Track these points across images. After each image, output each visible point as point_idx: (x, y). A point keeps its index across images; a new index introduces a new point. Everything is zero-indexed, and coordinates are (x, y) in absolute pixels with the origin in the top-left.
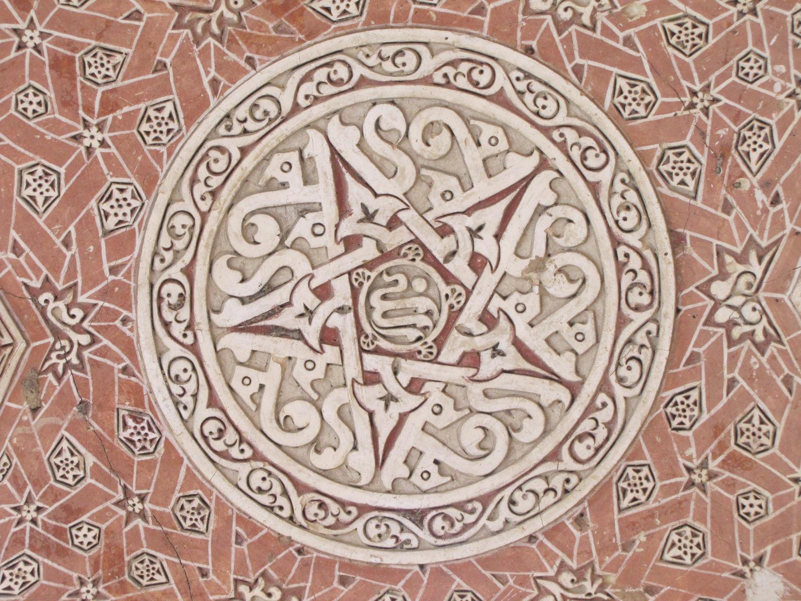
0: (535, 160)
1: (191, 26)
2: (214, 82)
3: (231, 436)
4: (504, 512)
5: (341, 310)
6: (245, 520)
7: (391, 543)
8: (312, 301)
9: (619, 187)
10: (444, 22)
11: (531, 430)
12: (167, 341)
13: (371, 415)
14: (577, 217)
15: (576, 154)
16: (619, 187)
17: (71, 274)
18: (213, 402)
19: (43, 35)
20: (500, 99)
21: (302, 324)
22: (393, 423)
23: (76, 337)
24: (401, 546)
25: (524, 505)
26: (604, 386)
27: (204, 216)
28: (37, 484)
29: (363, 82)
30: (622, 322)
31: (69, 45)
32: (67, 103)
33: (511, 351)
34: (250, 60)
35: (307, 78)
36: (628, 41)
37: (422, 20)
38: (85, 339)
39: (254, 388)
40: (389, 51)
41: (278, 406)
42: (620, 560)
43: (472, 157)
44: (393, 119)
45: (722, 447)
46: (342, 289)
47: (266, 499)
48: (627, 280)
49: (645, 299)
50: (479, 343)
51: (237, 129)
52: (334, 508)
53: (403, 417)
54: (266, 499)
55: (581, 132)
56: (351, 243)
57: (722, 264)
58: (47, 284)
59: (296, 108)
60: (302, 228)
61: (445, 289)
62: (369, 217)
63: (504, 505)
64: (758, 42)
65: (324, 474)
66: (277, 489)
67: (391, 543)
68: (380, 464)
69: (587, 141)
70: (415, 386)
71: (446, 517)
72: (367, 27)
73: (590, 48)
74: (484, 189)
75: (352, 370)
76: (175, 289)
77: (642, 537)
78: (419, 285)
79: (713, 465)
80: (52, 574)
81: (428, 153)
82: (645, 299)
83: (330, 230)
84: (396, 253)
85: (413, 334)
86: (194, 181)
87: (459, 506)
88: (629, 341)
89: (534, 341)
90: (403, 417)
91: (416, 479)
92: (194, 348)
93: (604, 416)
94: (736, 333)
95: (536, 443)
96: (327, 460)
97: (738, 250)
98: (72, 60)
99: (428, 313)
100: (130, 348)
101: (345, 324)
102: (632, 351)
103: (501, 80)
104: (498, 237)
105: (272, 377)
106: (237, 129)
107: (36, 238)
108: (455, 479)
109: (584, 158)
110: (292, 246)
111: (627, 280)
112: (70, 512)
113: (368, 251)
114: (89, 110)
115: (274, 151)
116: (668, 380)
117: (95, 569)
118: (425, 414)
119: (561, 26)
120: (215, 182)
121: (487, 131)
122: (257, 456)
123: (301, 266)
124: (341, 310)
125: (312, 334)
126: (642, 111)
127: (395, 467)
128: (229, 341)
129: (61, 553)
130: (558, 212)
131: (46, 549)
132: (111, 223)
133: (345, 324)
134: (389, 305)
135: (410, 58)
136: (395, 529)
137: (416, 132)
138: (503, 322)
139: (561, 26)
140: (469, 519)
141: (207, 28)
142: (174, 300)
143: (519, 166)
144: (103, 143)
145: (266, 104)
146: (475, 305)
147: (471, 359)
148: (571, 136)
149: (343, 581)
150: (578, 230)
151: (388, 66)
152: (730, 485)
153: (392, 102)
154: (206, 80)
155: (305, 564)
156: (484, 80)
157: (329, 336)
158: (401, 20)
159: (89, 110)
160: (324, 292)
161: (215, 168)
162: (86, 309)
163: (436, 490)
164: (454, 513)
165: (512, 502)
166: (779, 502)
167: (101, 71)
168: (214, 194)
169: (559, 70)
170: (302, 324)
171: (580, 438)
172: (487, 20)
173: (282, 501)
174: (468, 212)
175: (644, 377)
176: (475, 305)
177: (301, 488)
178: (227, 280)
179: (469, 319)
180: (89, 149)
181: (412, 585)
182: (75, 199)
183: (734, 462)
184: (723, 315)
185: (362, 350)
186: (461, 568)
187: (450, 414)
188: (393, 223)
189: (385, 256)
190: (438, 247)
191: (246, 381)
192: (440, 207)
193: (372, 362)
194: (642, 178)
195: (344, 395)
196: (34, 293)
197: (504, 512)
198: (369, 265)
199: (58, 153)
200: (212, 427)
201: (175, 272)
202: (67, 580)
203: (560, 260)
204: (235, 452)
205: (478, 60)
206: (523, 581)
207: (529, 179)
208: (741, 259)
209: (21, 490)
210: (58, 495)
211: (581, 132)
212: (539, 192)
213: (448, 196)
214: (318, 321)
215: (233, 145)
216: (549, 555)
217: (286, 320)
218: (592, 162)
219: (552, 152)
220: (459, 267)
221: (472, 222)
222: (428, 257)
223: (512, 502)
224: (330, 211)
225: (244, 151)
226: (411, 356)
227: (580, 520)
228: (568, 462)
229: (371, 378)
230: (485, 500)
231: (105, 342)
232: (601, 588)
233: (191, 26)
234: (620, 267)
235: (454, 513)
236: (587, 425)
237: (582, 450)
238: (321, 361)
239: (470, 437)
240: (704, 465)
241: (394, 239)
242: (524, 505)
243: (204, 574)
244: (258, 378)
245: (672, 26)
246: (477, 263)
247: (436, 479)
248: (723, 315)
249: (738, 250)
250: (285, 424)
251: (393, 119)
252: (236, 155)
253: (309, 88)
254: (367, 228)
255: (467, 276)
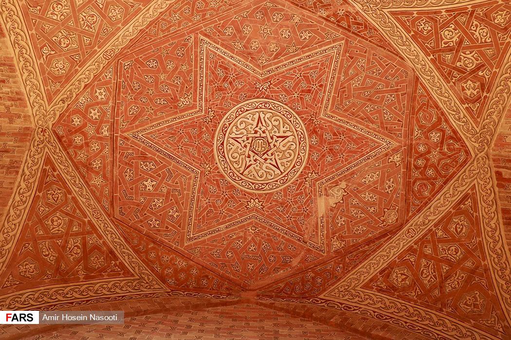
0: (283, 171)
1: (313, 115)
2: (303, 117)
3: (240, 113)
4: (222, 159)
5: (260, 134)
6: (226, 114)
7: (218, 139)
8: (262, 130)
9: (276, 185)
10: (309, 158)
11: (236, 166)
12: (259, 103)
13: (241, 138)
14: (272, 178)
15: (283, 178)
16: (276, 185)
17: (272, 88)
18: (247, 110)
19: (315, 89)
20: (294, 166)
21: (259, 127)
22: (239, 141)
23: (261, 87)
24: (217, 140)
25: (222, 163)
26: (242, 179)
27: (280, 113)
28: (236, 78)
29: (300, 143)
30: (253, 184)
31: (312, 93)
32: (303, 91)
33: (250, 163)
34: (306, 124)
35: (302, 134)
36: (301, 189)
37: (309, 154)
38: (261, 89)
39: (248, 118)
40: (305, 148)
41: (245, 122)
42: (211, 178)
43: (285, 161)
44: (293, 147)
45: (229, 198)
46: (264, 135)
47: (229, 118)
48: (260, 185)
49: (256, 188)
50: (252, 158)
51: (294, 120)
52: (226, 129)
53: (240, 143)
54: (229, 118)
55: (287, 180)
56: (272, 138)
57: (261, 201)
58: (271, 84)
59: (297, 131)
60: (276, 129)
61: (262, 153)
62: (276, 141)
63: (223, 159)
64: (299, 211)
65: (232, 128)
66: (230, 120)
67: (218, 139)
68: (232, 138)
69: (285, 180)
70: (245, 146)
71: (222, 149)
72: (310, 145)
73: (301, 183)
74: (279, 162)
75: (249, 135)
76: (268, 106)
77: (215, 182)
78: (263, 149)
79: (226, 196)
80: (220, 79)
81: (286, 153)
82: (256, 188)
83: (275, 134)
84: (269, 146)
85: (255, 147)
86: (286, 112)
87: (223, 152)
88: (249, 185)
89: (251, 168)
90: (240, 143)
91: (229, 144)
92: (257, 108)
93: (237, 179)
94: (249, 203)
95: (233, 166)
96: (234, 129)
97: (263, 204)
98: (310, 93)
99: (258, 150)
100: (258, 97)
101: (258, 135)
102: (248, 184)
103: (297, 167)
104: (270, 164)
105: (250, 121)
106: (294, 120)
107: (279, 83)
108: (228, 151)
109: (282, 180)
110: (273, 127)
111: (260, 185)
112: (231, 83)
113: (270, 140)
114: (301, 95)
115: (290, 126)
116: (242, 191)
117: (220, 86)
118: (240, 147)
119: (305, 178)
120: (286, 115)
121: (289, 164)
122: (236, 117)
123: (269, 128)
124: (260, 134)
125: (257, 129)
126: (289, 190)
127: (232, 141)
128: (257, 114)
129: (224, 81)
130: (273, 174)
131: (225, 78)
132: (280, 96)
133: (258, 135)
134: (260, 143)
135: (303, 152)
136: (220, 140)
137: (290, 151)
138: (255, 163)
139: (305, 178)
140: (221, 153)
141: (312, 117)
142: (266, 106)
143: (282, 168)
144: (295, 97)
145: (298, 125)
146: (258, 158)
147: (249, 157)
148: (286, 178)
149: (212, 130)
150: (270, 177)
151: (302, 148)
152: (223, 199)
153: (296, 147)
154: (303, 116)
155: (216, 123)
156: (298, 164)
157: (256, 132)
158: (310, 150)
159: (301, 95)
160: (264, 132)
161: (288, 116)
162: (266, 90)
163: (227, 148)
164: (222, 150)
165: (223, 161)
166: (219, 207)
167: (308, 98)
168: (283, 115)
169: (298, 177)
170: (259, 127)
171: (233, 174)
172: (308, 166)
173: (228, 120)
174: (275, 159)
175: (243, 186)
176: (258, 158)
177: (230, 124)
178: (268, 115)
179: (256, 157)
180: (294, 94)
181: (210, 142)
182: (286, 90)
183: (227, 200)
184: (252, 200)
185: (253, 137)
186: (212, 150)
187: (240, 151)
188: (275, 146)
189: (269, 143)
190: (269, 153)
191: (250, 116)
192: (276, 154)
193: (251, 139)
194: (278, 189)
195: (245, 134)
196: (270, 82)
197: (222, 159)
198: (268, 141)
199: (294, 88)
200: (243, 109)
201: (271, 106)
202: (219, 81)
203: (265, 174)
204: (238, 113)
205: (301, 164)
206: (209, 161)
207: (280, 170)
208: (262, 205)
209: (236, 75)
210: (234, 81)
211: (287, 180)
212: (277, 171)
213: (278, 155)
214: (259, 130)
215: (292, 119)
216: (214, 166)
217: (260, 124)
218: (281, 181)
219: (284, 174)
220: (265, 156)
221: (273, 159)
222: (268, 151)
223: (223, 161)
224: (277, 134)
225: (290, 121)
226: (251, 146)
227: (218, 172)
228: (229, 171)
229: (248, 139)
230: (224, 156)
231: (260, 93)
232: (207, 175)
233: (313, 115)
234: (262, 184)
235: (222, 150)
236: (235, 175)
237: (231, 174)
238: (252, 130)
239: (235, 155)
240: (226, 195)
241: (272, 145)
242: (222, 163)
243: (217, 105)
244: (250, 119)
245: (303, 197)
246: (266, 159)
247: (229, 148)
248: (252, 200)
249: (263, 204)
250: (241, 123)
251: (293, 147)
252: (290, 119)
253: (300, 134)
254: (274, 140)
255: (263, 157)
